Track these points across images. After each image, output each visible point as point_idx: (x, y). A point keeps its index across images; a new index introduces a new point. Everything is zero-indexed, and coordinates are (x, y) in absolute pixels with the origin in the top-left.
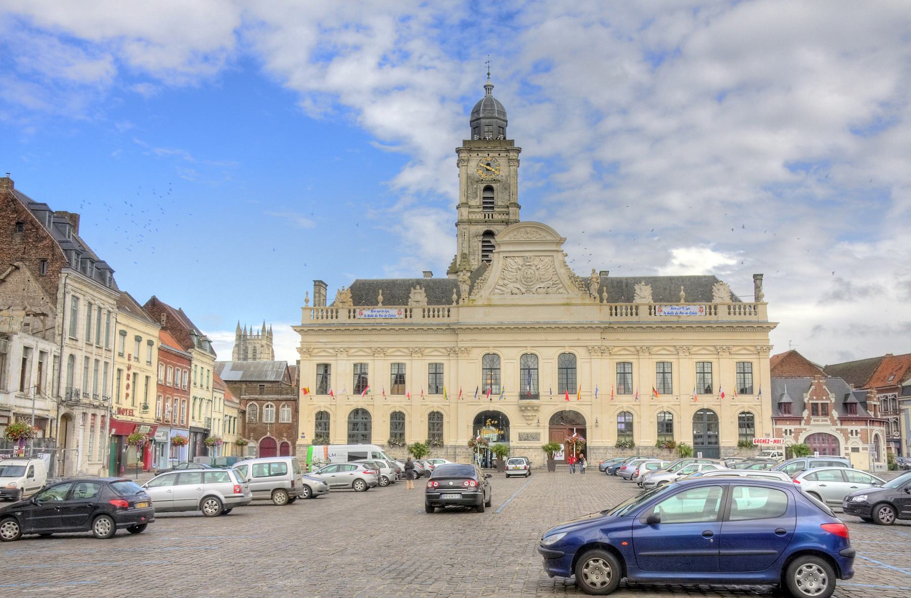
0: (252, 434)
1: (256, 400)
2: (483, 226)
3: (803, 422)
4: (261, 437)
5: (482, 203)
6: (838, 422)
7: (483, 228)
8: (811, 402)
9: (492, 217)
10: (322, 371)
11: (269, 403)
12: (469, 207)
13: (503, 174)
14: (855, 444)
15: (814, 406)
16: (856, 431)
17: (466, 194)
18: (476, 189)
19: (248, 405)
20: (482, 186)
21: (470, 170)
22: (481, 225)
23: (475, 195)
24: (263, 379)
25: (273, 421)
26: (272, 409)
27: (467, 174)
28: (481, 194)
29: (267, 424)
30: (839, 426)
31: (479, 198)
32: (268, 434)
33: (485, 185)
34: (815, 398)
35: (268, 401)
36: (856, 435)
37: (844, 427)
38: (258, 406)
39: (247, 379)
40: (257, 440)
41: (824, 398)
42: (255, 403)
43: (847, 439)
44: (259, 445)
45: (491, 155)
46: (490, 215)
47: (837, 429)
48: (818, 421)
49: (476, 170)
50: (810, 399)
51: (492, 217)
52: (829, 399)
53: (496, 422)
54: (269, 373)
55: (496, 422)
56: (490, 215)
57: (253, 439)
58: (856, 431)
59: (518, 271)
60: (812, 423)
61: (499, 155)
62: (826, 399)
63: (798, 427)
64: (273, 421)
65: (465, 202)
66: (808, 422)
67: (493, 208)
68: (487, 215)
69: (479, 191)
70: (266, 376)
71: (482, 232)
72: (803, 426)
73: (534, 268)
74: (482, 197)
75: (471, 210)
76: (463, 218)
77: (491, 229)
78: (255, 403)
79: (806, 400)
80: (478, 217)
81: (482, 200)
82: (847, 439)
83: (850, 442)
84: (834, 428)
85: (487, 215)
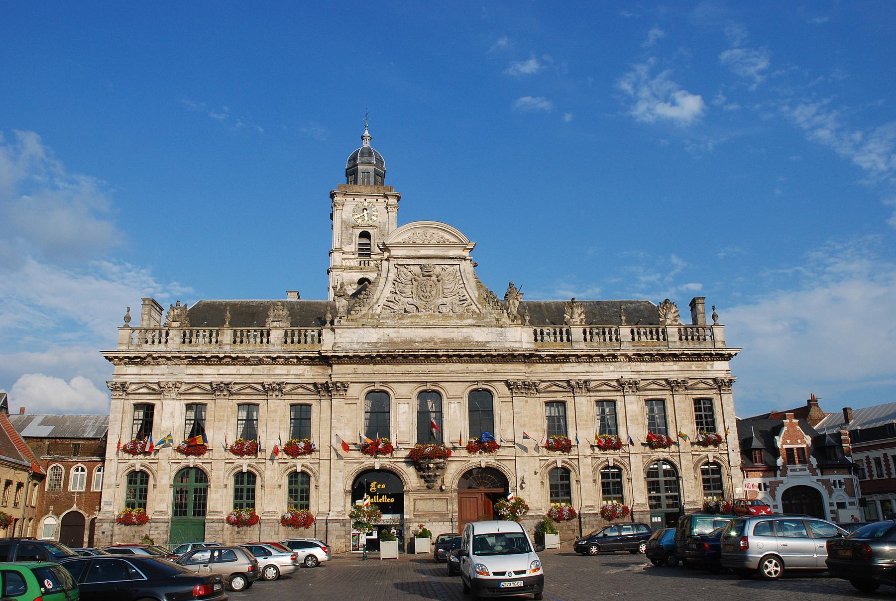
0: (52, 508)
1: (61, 461)
2: (358, 274)
3: (779, 472)
4: (64, 512)
5: (357, 249)
6: (818, 471)
7: (358, 276)
8: (785, 447)
9: (369, 265)
10: (141, 414)
11: (79, 464)
12: (343, 253)
13: (381, 220)
14: (841, 497)
15: (790, 451)
16: (839, 481)
17: (340, 239)
18: (352, 234)
19: (50, 468)
20: (358, 232)
21: (345, 215)
22: (356, 272)
23: (350, 241)
24: (79, 435)
25: (84, 490)
26: (83, 473)
27: (342, 219)
28: (356, 240)
29: (73, 493)
30: (819, 477)
31: (354, 244)
32: (75, 508)
33: (361, 231)
34: (788, 441)
35: (77, 462)
36: (840, 487)
37: (825, 477)
38: (63, 469)
39: (57, 436)
40: (58, 515)
41: (799, 441)
42: (60, 465)
43: (831, 492)
44: (60, 522)
45: (368, 200)
46: (366, 262)
47: (818, 480)
48: (795, 470)
49: (351, 215)
50: (784, 443)
51: (369, 265)
52: (805, 443)
53: (384, 486)
54: (89, 429)
55: (384, 486)
56: (366, 262)
57: (53, 513)
58: (839, 481)
59: (414, 281)
60: (789, 473)
61: (377, 200)
62: (802, 443)
63: (773, 479)
64: (84, 490)
65: (339, 247)
66: (784, 474)
67: (369, 255)
68: (362, 262)
69: (354, 236)
70: (84, 432)
71: (356, 280)
72: (779, 478)
73: (434, 278)
74: (357, 243)
75: (344, 256)
76: (336, 264)
77: (367, 276)
78: (60, 465)
79: (779, 445)
80: (352, 264)
81: (357, 247)
82: (831, 492)
83: (834, 495)
84: (815, 478)
85: (362, 262)
